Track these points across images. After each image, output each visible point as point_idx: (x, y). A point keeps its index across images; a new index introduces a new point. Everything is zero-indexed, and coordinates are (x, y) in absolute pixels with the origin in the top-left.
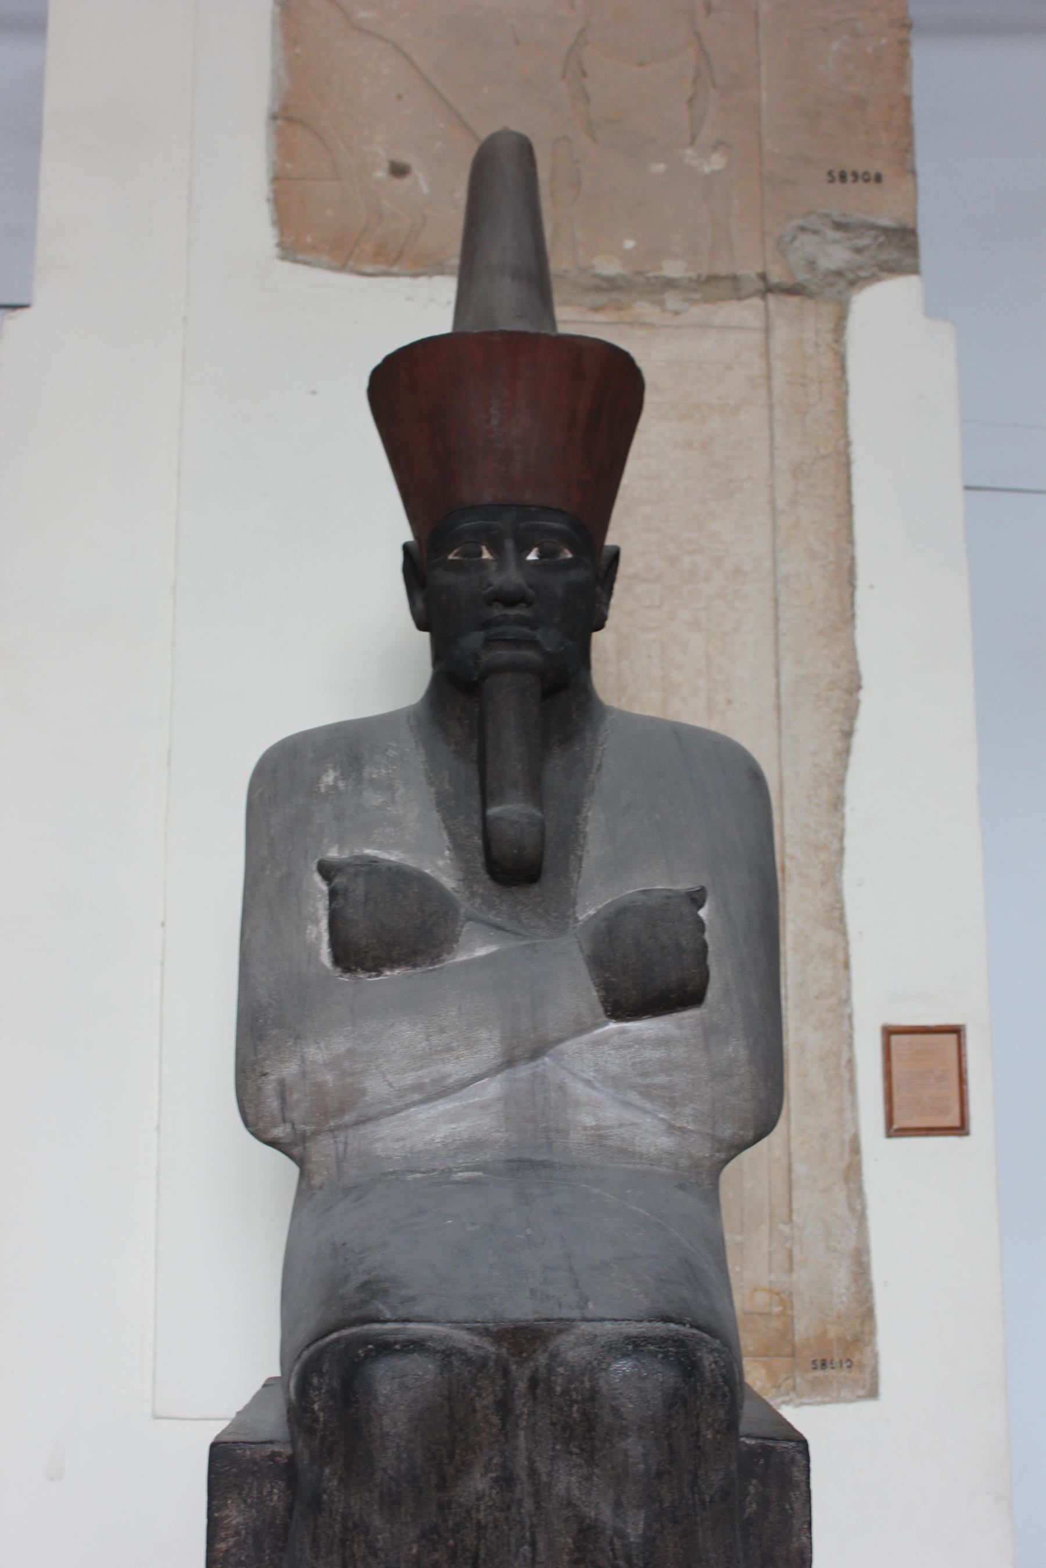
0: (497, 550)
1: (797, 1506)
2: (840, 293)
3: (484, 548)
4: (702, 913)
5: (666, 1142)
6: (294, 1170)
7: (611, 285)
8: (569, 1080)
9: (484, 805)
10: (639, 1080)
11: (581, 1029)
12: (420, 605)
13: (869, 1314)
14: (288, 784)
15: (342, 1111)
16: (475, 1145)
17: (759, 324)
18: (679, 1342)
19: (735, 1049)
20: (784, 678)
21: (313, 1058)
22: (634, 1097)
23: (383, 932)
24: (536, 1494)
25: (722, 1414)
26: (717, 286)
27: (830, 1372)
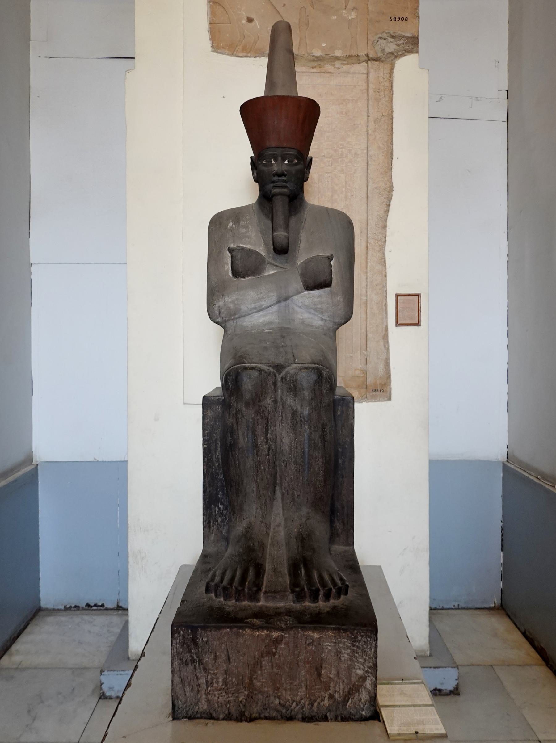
1: (351, 413)
2: (392, 60)
4: (332, 262)
5: (321, 323)
6: (223, 330)
7: (318, 59)
8: (295, 307)
10: (313, 307)
11: (298, 293)
12: (255, 174)
13: (389, 377)
15: (235, 314)
16: (270, 323)
17: (365, 72)
18: (317, 369)
19: (339, 298)
21: (227, 301)
22: (313, 311)
23: (245, 267)
24: (283, 405)
25: (328, 386)
27: (377, 393)
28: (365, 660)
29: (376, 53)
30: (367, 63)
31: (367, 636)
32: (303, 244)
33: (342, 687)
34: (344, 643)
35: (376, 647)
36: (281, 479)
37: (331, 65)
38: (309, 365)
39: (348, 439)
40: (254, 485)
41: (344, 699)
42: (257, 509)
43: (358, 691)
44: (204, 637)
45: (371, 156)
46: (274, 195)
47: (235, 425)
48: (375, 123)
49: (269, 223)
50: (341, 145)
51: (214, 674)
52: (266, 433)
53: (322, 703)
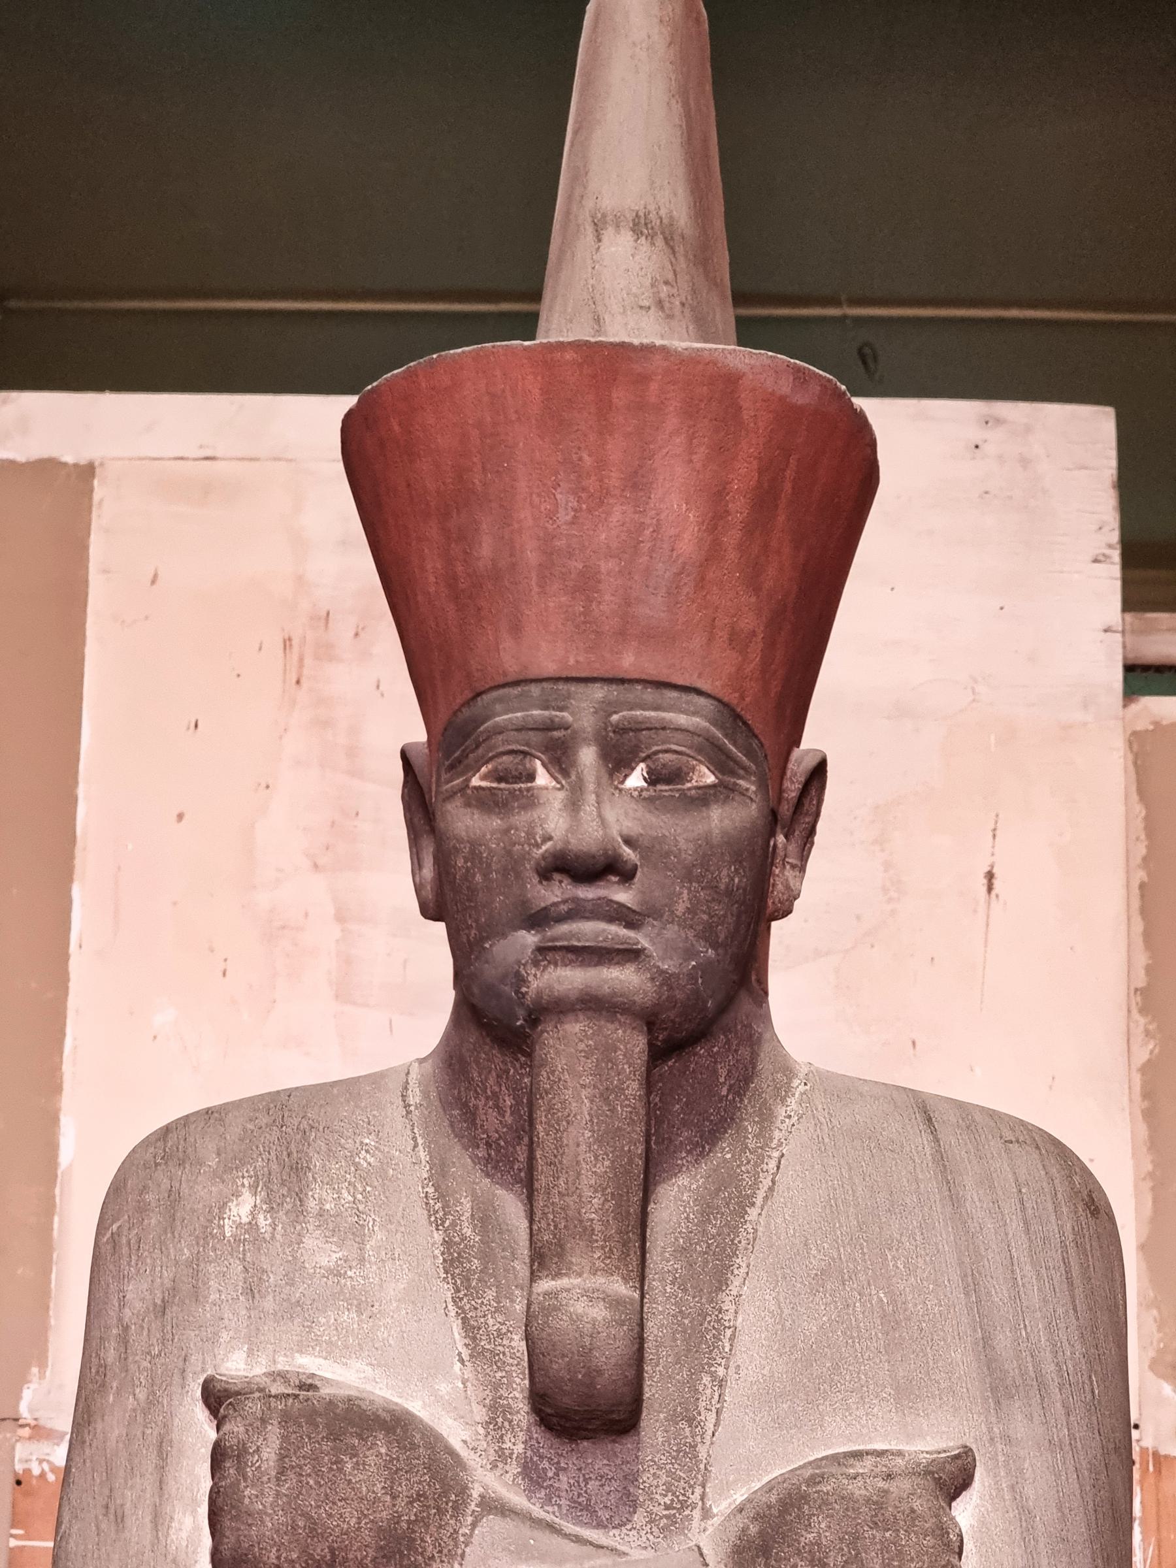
3: (538, 763)
9: (533, 1277)
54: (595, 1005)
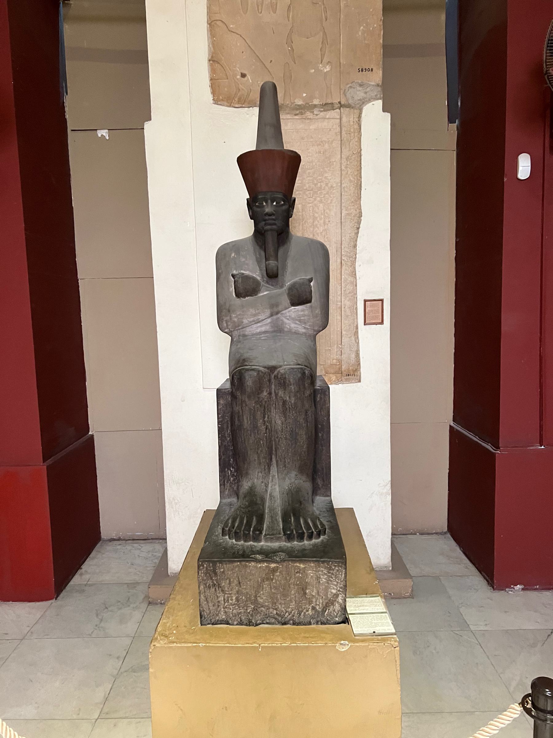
0: (266, 202)
5: (304, 331)
7: (299, 107)
11: (286, 309)
14: (224, 256)
15: (239, 326)
17: (338, 117)
18: (302, 368)
19: (318, 311)
20: (343, 215)
22: (298, 322)
23: (246, 289)
26: (327, 106)
28: (338, 582)
29: (347, 100)
30: (340, 109)
31: (339, 566)
32: (289, 269)
33: (321, 601)
34: (322, 571)
35: (346, 573)
36: (276, 451)
37: (311, 112)
38: (295, 366)
39: (326, 418)
40: (256, 456)
41: (323, 610)
42: (258, 473)
43: (333, 604)
44: (221, 568)
45: (344, 188)
46: (266, 231)
47: (241, 412)
48: (347, 160)
49: (263, 253)
50: (320, 179)
51: (229, 594)
52: (264, 417)
53: (307, 613)
54: (271, 230)
